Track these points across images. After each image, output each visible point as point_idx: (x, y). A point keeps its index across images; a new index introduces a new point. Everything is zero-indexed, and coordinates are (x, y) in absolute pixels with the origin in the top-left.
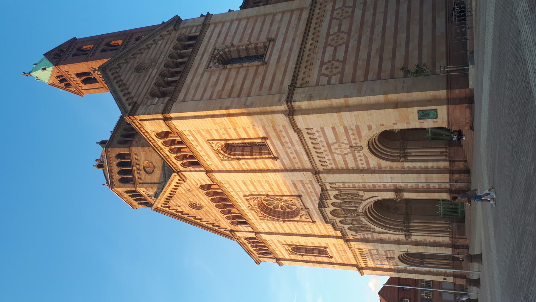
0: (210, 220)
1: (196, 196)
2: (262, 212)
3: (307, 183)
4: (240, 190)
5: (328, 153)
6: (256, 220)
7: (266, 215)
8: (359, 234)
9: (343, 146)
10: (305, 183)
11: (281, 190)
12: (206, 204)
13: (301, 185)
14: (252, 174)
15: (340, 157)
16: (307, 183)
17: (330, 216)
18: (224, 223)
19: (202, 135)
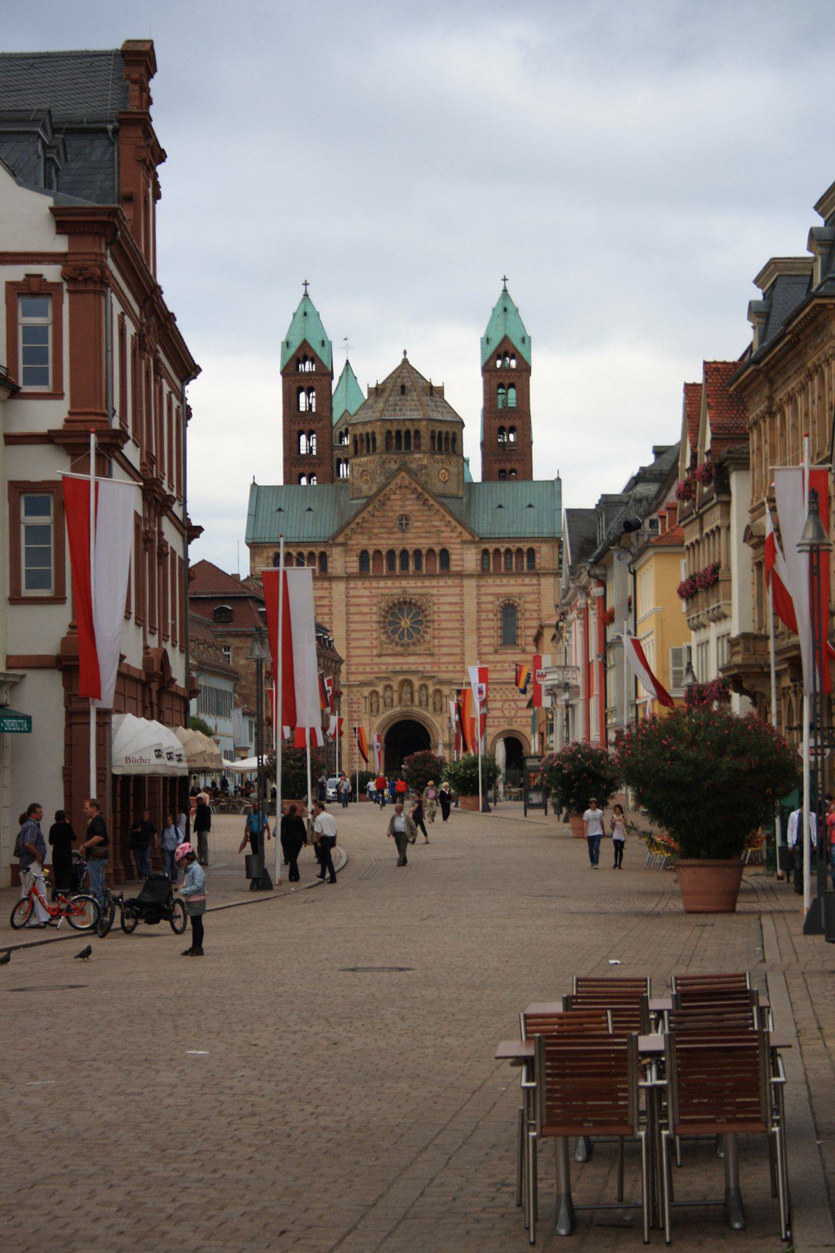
0: (371, 526)
2: (396, 601)
3: (454, 667)
4: (441, 593)
5: (504, 697)
6: (378, 588)
7: (391, 604)
8: (358, 699)
9: (513, 713)
11: (443, 638)
14: (475, 620)
15: (500, 706)
16: (454, 667)
17: (401, 678)
18: (365, 542)
19: (529, 593)
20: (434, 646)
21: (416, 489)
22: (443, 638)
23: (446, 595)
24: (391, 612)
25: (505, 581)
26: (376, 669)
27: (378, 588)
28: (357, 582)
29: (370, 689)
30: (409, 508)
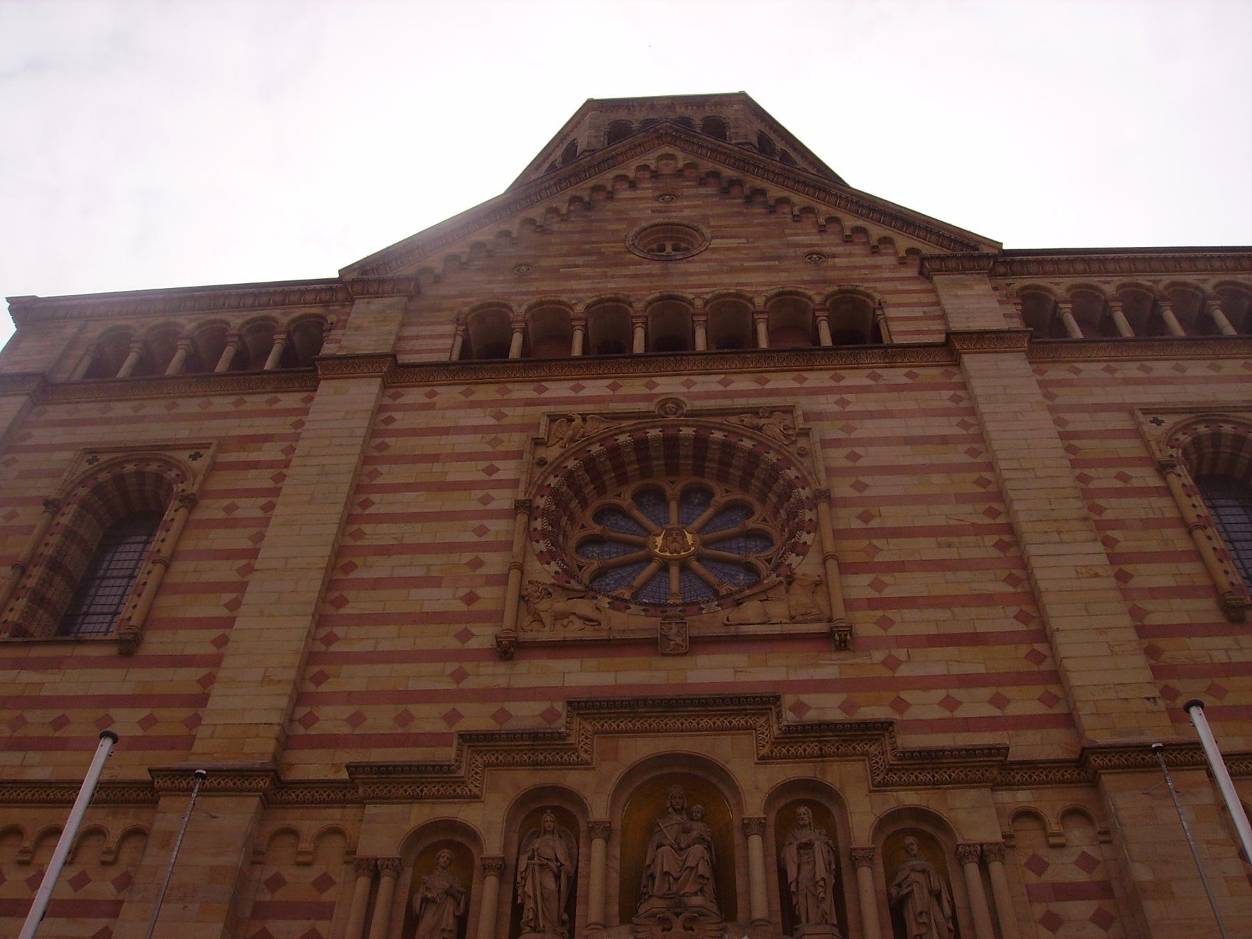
1: (760, 263)
2: (623, 438)
3: (999, 701)
4: (850, 408)
8: (324, 882)
10: (1008, 692)
11: (900, 566)
12: (692, 274)
13: (981, 669)
17: (640, 748)
20: (849, 605)
21: (715, 175)
22: (900, 566)
23: (887, 414)
24: (595, 504)
25: (1162, 368)
26: (477, 718)
27: (529, 403)
28: (437, 389)
29: (419, 814)
30: (687, 213)
